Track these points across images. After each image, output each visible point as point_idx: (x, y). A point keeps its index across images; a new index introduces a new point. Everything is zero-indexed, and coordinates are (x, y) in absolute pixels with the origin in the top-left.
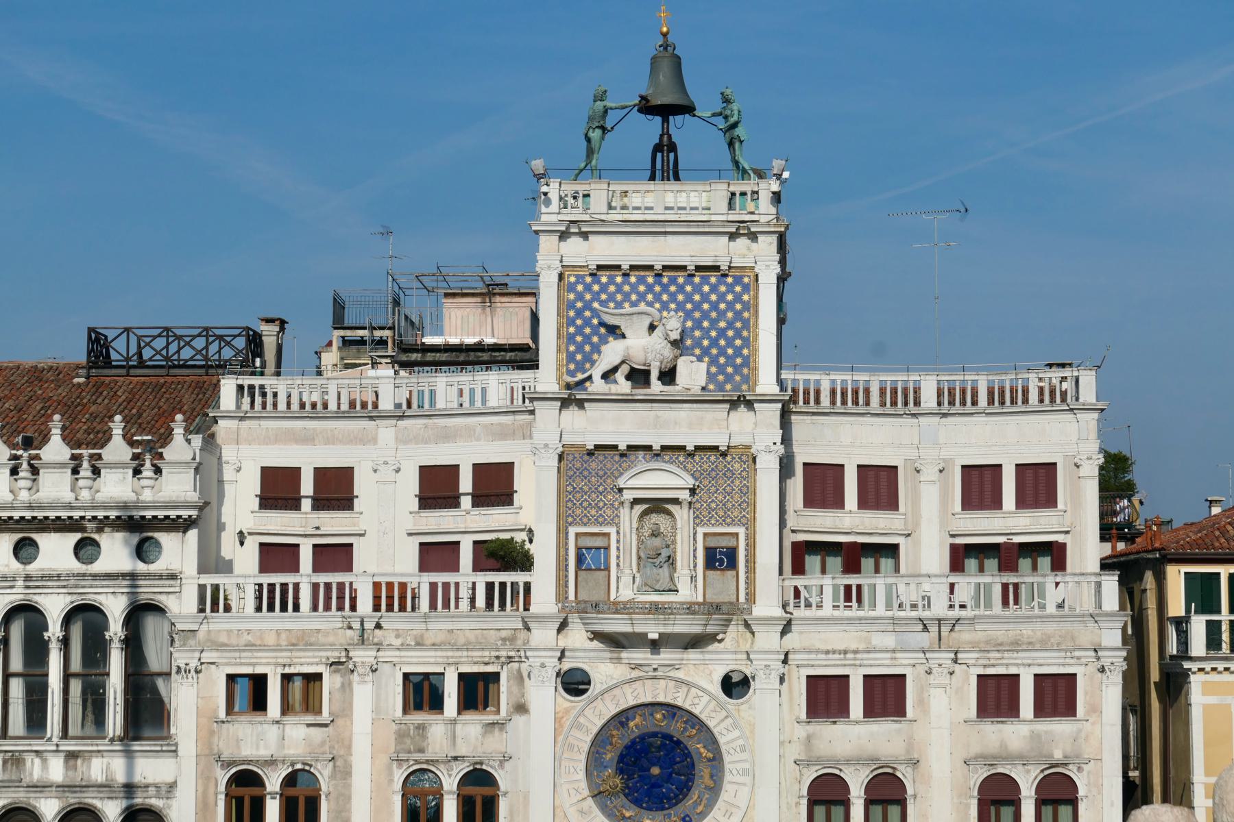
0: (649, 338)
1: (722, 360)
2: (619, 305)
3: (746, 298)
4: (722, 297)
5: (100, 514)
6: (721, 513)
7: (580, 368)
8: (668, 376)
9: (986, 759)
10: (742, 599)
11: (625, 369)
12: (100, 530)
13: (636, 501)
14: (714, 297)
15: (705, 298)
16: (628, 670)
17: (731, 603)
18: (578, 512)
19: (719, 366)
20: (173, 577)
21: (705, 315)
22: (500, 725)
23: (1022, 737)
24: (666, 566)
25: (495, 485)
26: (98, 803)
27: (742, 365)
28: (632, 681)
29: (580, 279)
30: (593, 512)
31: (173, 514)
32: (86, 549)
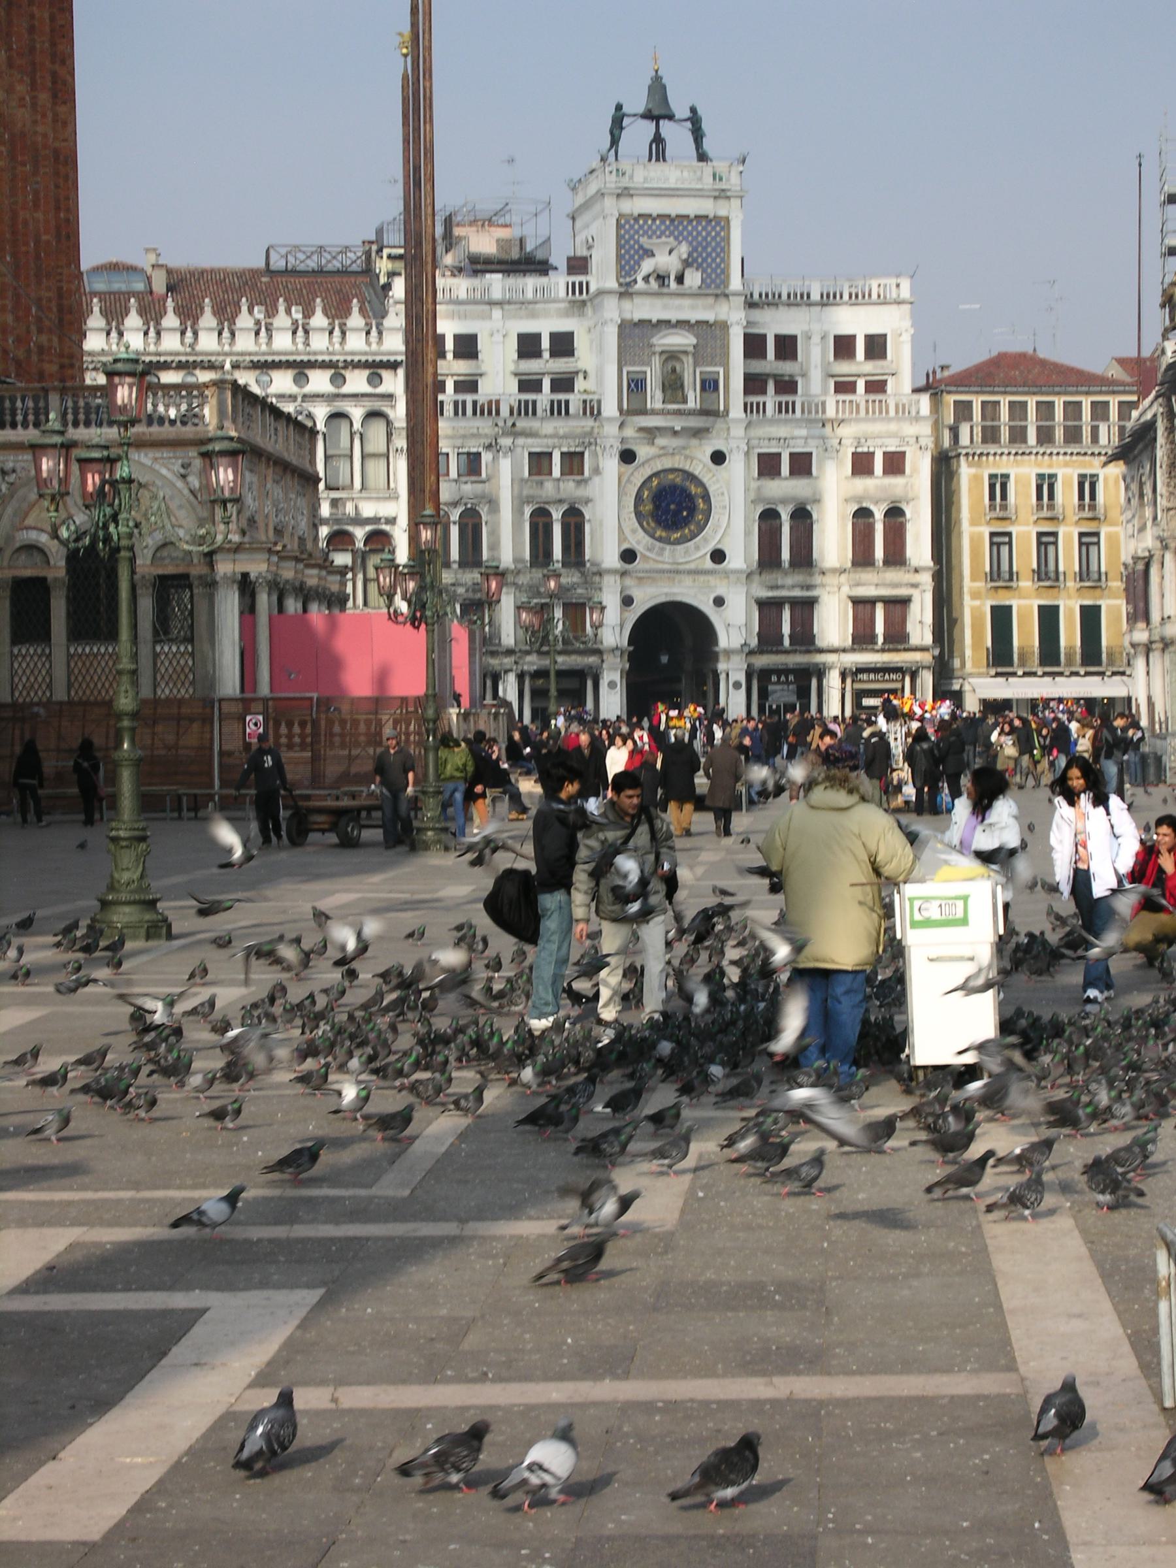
2: (650, 237)
4: (708, 234)
5: (349, 358)
7: (628, 274)
8: (680, 279)
9: (859, 499)
12: (345, 368)
13: (662, 352)
15: (699, 233)
20: (390, 397)
22: (586, 481)
23: (877, 487)
25: (563, 345)
26: (350, 528)
28: (659, 456)
29: (627, 222)
31: (392, 359)
32: (338, 379)
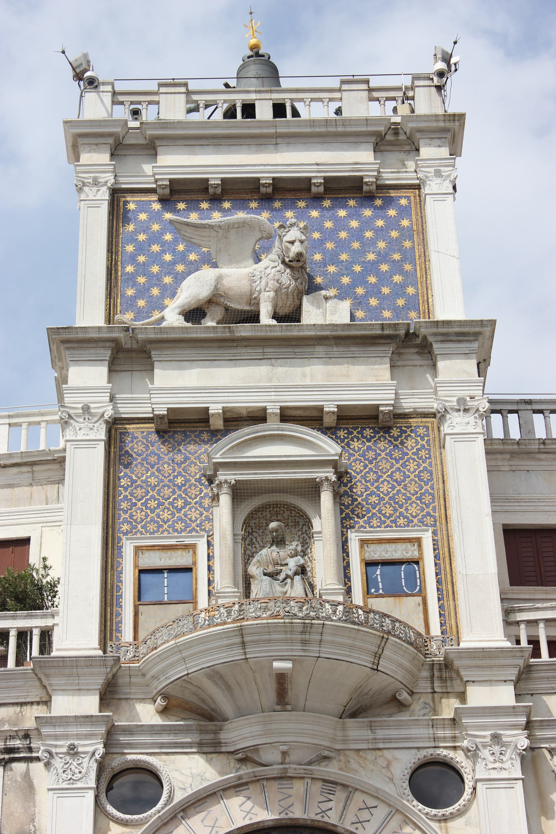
0: (256, 265)
1: (373, 302)
3: (405, 223)
4: (367, 224)
6: (388, 511)
10: (435, 630)
11: (219, 313)
14: (354, 224)
16: (232, 764)
17: (420, 634)
18: (139, 516)
19: (368, 309)
21: (343, 245)
24: (297, 578)
27: (407, 307)
30: (166, 515)
